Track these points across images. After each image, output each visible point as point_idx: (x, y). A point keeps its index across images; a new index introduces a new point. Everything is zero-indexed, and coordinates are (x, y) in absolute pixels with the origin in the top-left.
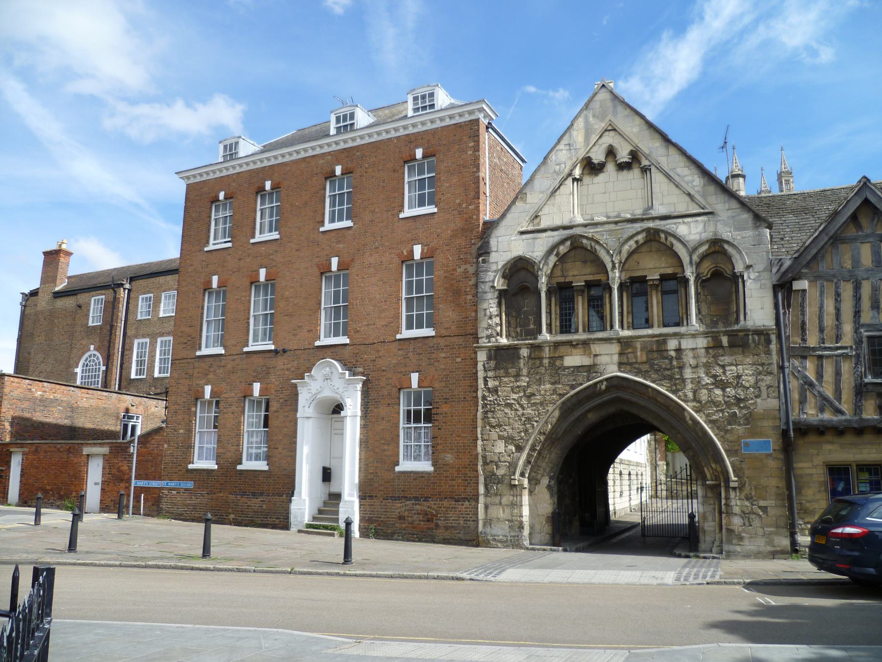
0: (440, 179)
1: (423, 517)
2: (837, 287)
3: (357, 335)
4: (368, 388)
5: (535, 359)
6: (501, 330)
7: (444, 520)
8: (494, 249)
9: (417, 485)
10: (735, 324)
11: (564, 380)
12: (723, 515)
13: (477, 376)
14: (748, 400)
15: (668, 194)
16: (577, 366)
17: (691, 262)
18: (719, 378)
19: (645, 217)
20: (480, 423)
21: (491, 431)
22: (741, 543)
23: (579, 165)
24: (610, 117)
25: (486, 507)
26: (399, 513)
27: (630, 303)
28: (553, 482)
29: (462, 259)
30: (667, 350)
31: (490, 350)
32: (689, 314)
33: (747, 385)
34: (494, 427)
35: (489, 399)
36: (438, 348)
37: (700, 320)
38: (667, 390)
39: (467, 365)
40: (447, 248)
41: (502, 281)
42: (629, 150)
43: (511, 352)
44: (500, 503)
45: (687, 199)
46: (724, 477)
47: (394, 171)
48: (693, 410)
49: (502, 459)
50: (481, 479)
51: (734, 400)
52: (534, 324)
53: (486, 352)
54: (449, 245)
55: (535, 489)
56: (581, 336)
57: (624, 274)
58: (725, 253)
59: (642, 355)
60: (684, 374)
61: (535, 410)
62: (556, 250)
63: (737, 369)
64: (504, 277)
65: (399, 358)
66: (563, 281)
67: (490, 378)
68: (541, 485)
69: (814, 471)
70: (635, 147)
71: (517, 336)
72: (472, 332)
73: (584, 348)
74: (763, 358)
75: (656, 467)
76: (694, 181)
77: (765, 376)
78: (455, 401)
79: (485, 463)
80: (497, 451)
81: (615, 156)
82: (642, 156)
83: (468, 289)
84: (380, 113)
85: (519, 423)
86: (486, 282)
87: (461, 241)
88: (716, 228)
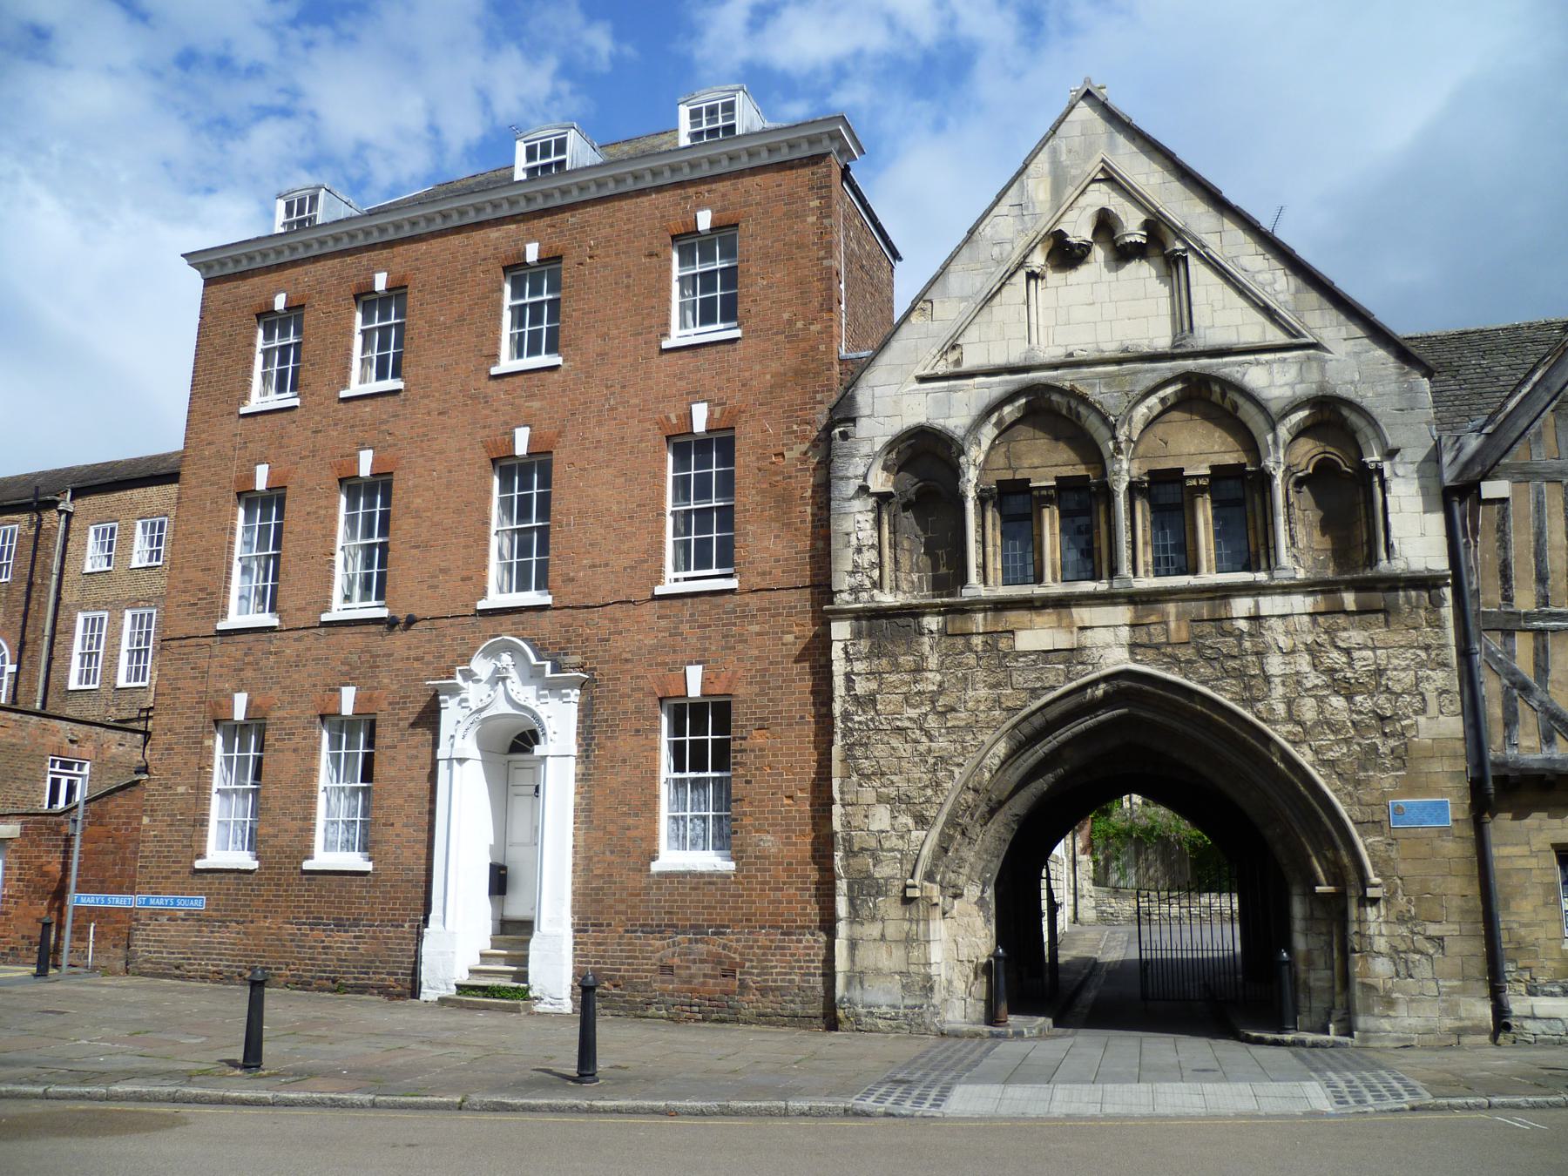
1: (713, 969)
3: (570, 588)
4: (592, 698)
7: (758, 975)
8: (866, 411)
9: (698, 901)
10: (1365, 566)
11: (1018, 678)
14: (1399, 720)
15: (1224, 308)
18: (1338, 676)
19: (1179, 351)
21: (861, 786)
22: (1391, 1013)
23: (1039, 246)
25: (853, 945)
26: (661, 960)
32: (1271, 545)
33: (1397, 688)
34: (868, 777)
35: (856, 718)
38: (1232, 700)
40: (764, 409)
41: (882, 475)
47: (651, 255)
48: (1289, 741)
49: (887, 845)
51: (1371, 718)
53: (848, 623)
54: (767, 404)
56: (1053, 587)
57: (1136, 464)
59: (1178, 628)
61: (955, 742)
63: (1376, 656)
67: (858, 674)
68: (965, 898)
69: (1533, 863)
73: (1059, 614)
74: (1428, 635)
76: (1275, 282)
77: (1432, 670)
78: (781, 724)
79: (850, 853)
80: (874, 827)
82: (1168, 231)
84: (612, 150)
85: (923, 769)
86: (849, 478)
87: (792, 396)
88: (1324, 376)
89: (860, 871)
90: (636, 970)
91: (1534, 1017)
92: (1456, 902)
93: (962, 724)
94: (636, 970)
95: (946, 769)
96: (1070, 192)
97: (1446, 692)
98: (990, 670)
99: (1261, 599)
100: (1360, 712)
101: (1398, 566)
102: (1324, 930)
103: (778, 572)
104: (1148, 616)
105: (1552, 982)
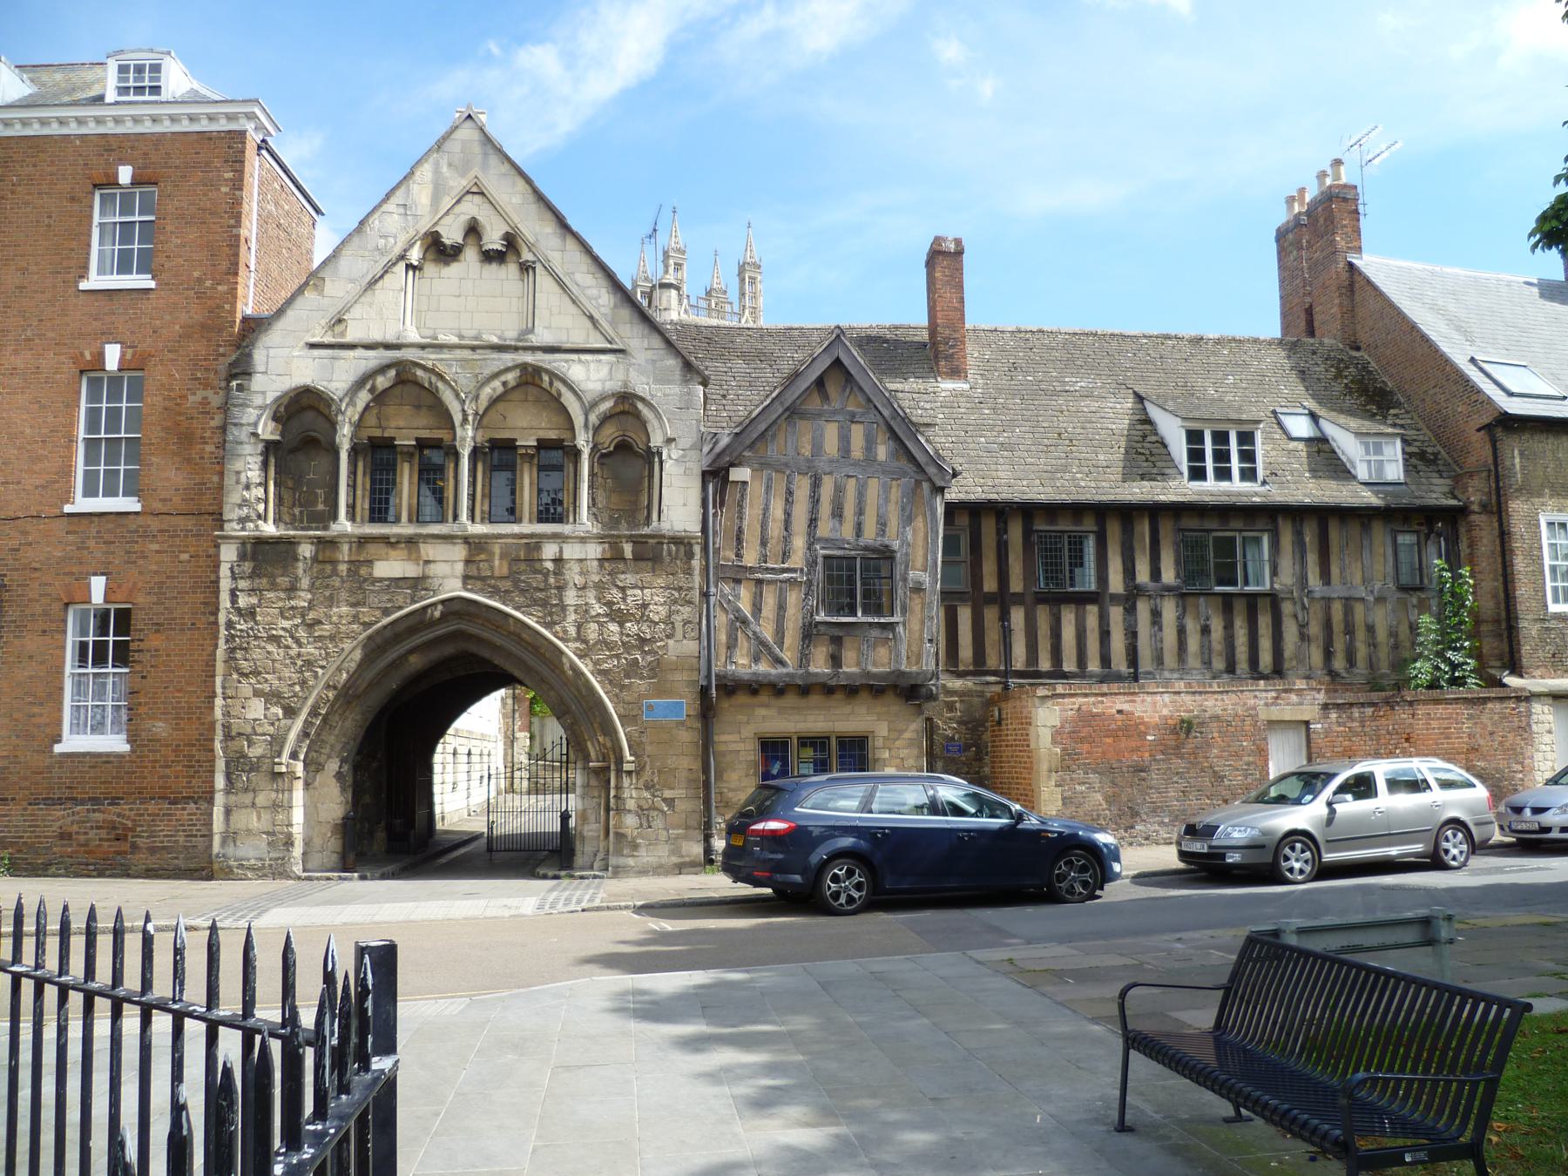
1: (108, 834)
2: (789, 482)
5: (324, 562)
7: (148, 837)
9: (96, 778)
11: (373, 599)
12: (611, 813)
13: (218, 587)
15: (560, 313)
17: (586, 425)
19: (521, 344)
20: (220, 667)
21: (240, 682)
24: (476, 171)
25: (228, 812)
26: (61, 828)
27: (487, 480)
28: (346, 768)
29: (199, 379)
30: (541, 560)
31: (243, 544)
33: (656, 619)
34: (246, 675)
35: (238, 627)
36: (146, 535)
37: (595, 516)
38: (537, 622)
39: (201, 567)
40: (171, 356)
41: (271, 425)
43: (282, 548)
44: (254, 805)
45: (588, 324)
46: (616, 758)
47: (73, 199)
48: (574, 653)
49: (259, 730)
50: (220, 765)
51: (636, 640)
52: (325, 502)
53: (235, 546)
54: (176, 351)
55: (314, 780)
56: (405, 529)
57: (480, 432)
58: (637, 415)
59: (501, 565)
60: (564, 599)
61: (320, 648)
62: (371, 382)
65: (69, 548)
67: (241, 591)
68: (325, 772)
69: (741, 746)
70: (513, 229)
71: (293, 523)
72: (211, 509)
73: (409, 550)
75: (512, 742)
78: (175, 629)
79: (228, 737)
80: (250, 716)
82: (525, 247)
83: (208, 434)
84: (45, 76)
85: (292, 670)
86: (242, 425)
87: (197, 347)
88: (628, 377)
90: (40, 837)
92: (683, 775)
93: (327, 634)
94: (36, 837)
95: (312, 671)
97: (690, 622)
98: (351, 592)
99: (565, 546)
100: (628, 635)
102: (596, 794)
103: (177, 500)
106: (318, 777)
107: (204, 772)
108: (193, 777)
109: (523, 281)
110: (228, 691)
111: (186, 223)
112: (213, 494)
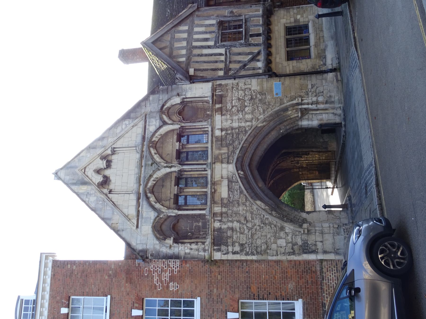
0: (87, 292)
6: (201, 242)
9: (314, 315)
11: (237, 197)
14: (252, 94)
15: (131, 138)
16: (228, 189)
17: (172, 124)
18: (239, 109)
21: (270, 249)
23: (101, 189)
24: (77, 170)
25: (325, 252)
30: (222, 136)
31: (214, 250)
32: (201, 127)
33: (243, 94)
38: (245, 136)
40: (138, 286)
42: (100, 160)
48: (257, 121)
52: (198, 222)
54: (136, 285)
58: (169, 108)
60: (236, 127)
64: (165, 239)
66: (173, 200)
67: (233, 250)
70: (99, 156)
71: (206, 234)
73: (217, 184)
74: (230, 87)
78: (249, 280)
79: (293, 253)
80: (285, 245)
81: (101, 169)
82: (106, 152)
88: (155, 112)
89: (300, 250)
91: (332, 64)
96: (86, 179)
97: (245, 83)
98: (234, 206)
99: (216, 128)
100: (250, 103)
101: (210, 94)
104: (219, 158)
105: (322, 61)
106: (309, 221)
107: (309, 266)
108: (311, 270)
109: (118, 153)
110: (274, 254)
111: (86, 283)
112: (194, 266)
